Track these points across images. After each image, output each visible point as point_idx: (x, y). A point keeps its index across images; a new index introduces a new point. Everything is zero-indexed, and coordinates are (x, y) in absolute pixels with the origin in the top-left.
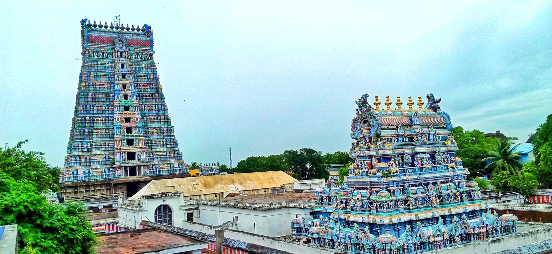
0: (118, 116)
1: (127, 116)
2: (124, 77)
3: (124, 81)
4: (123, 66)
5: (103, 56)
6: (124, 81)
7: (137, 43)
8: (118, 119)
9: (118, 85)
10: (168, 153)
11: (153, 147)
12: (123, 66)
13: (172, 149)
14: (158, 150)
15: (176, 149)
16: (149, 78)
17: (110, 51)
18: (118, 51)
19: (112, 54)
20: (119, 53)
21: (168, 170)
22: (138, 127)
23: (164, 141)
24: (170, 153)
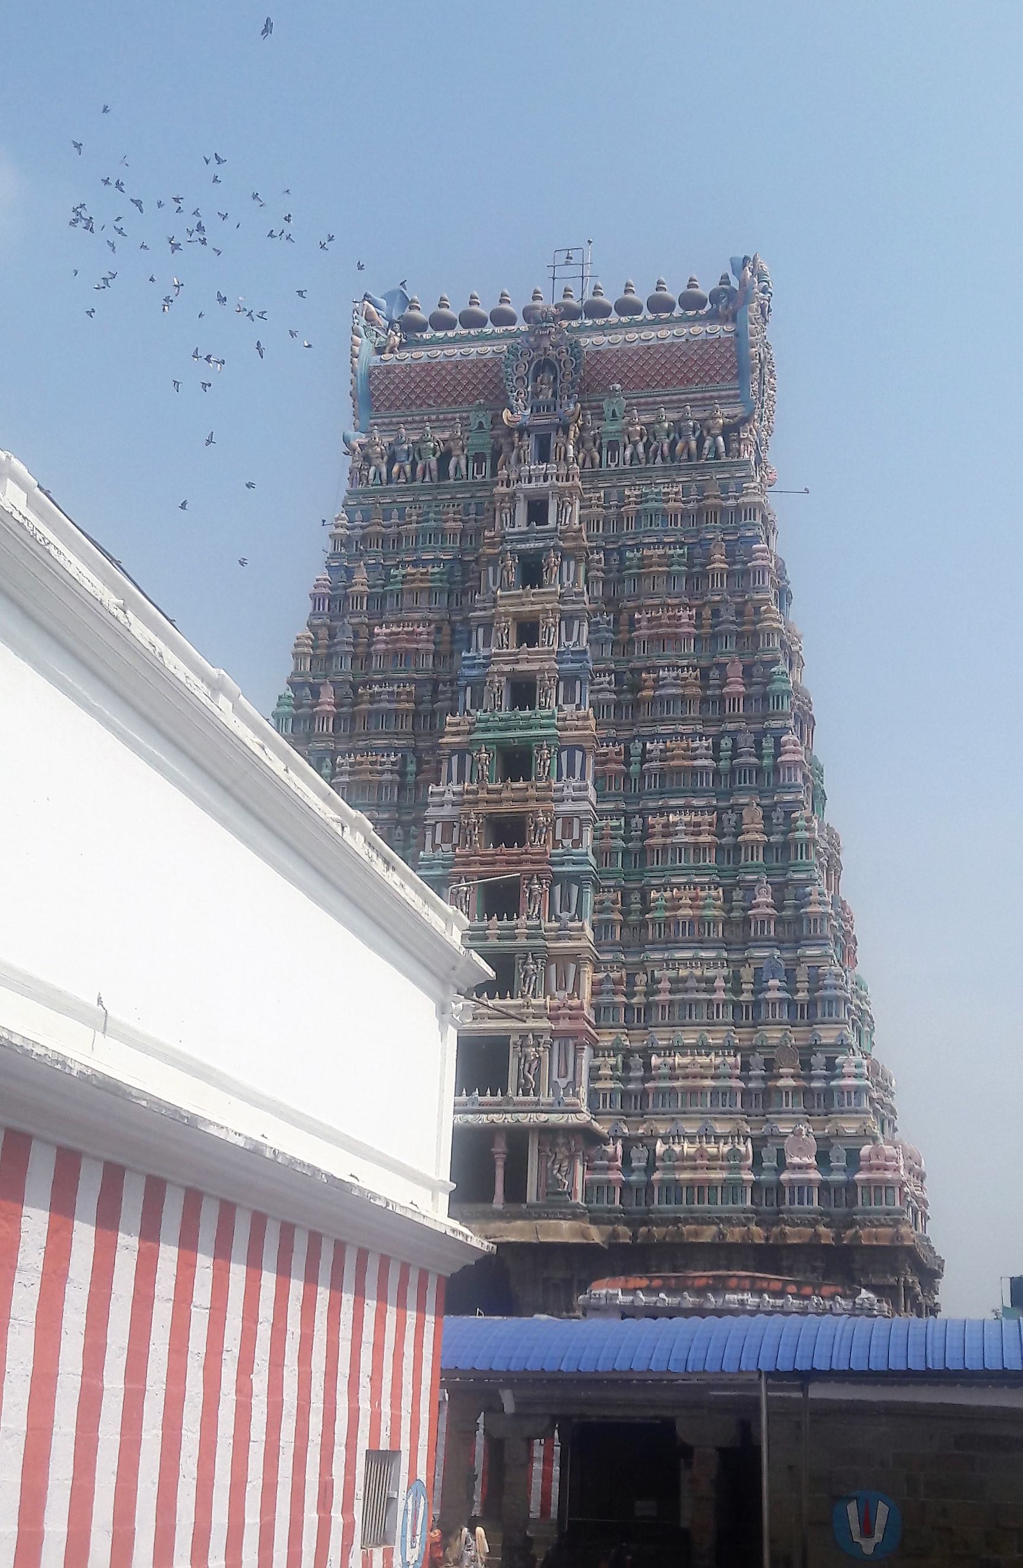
0: (447, 810)
1: (505, 808)
2: (532, 572)
3: (531, 602)
4: (537, 511)
5: (443, 473)
6: (531, 602)
7: (655, 372)
8: (448, 825)
9: (488, 625)
10: (757, 1059)
11: (657, 1016)
12: (537, 511)
13: (797, 1037)
14: (690, 1039)
15: (828, 1036)
16: (698, 577)
17: (482, 442)
18: (523, 430)
19: (496, 454)
20: (530, 444)
21: (733, 1188)
22: (556, 879)
23: (747, 973)
24: (769, 1064)
